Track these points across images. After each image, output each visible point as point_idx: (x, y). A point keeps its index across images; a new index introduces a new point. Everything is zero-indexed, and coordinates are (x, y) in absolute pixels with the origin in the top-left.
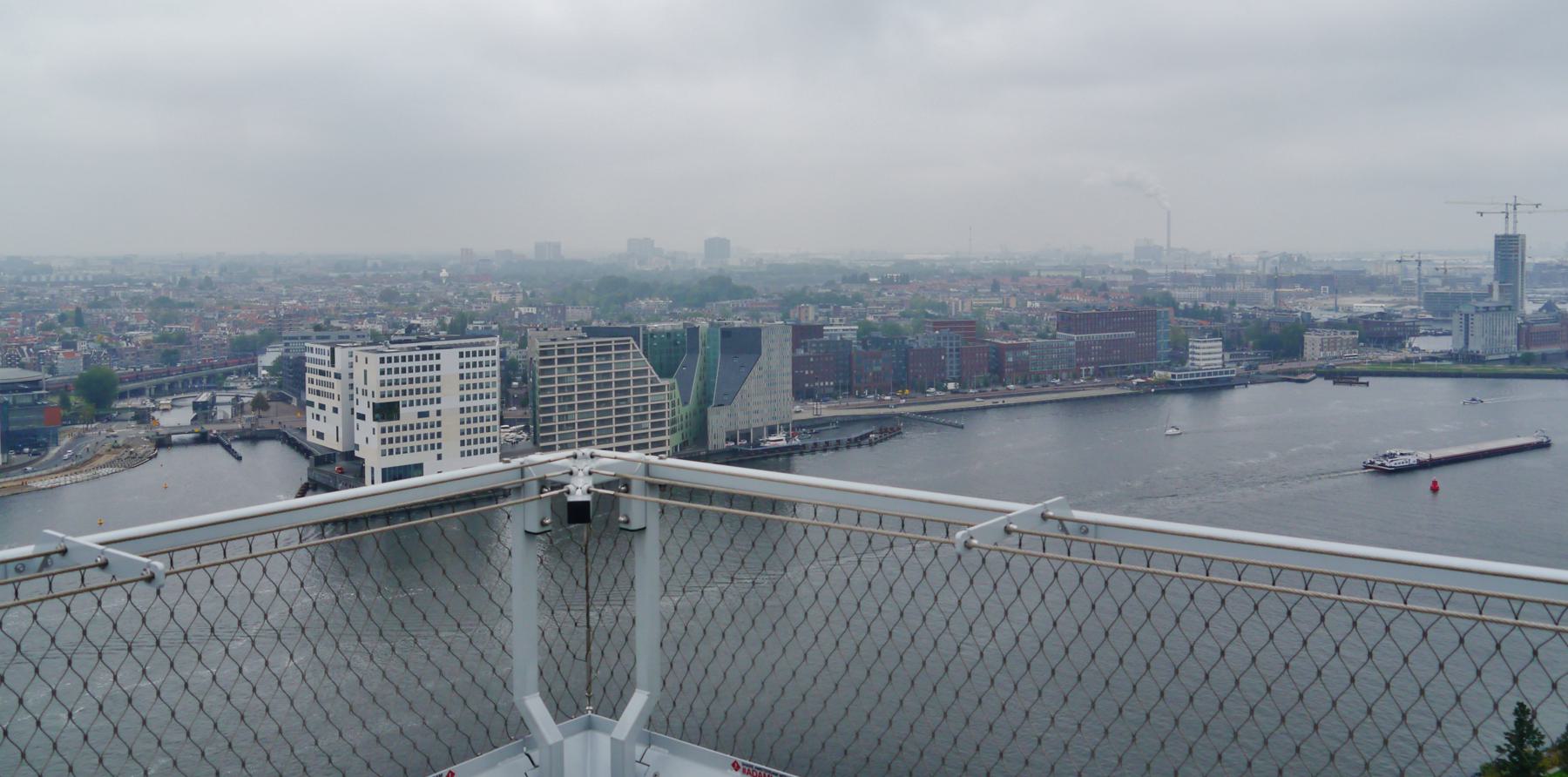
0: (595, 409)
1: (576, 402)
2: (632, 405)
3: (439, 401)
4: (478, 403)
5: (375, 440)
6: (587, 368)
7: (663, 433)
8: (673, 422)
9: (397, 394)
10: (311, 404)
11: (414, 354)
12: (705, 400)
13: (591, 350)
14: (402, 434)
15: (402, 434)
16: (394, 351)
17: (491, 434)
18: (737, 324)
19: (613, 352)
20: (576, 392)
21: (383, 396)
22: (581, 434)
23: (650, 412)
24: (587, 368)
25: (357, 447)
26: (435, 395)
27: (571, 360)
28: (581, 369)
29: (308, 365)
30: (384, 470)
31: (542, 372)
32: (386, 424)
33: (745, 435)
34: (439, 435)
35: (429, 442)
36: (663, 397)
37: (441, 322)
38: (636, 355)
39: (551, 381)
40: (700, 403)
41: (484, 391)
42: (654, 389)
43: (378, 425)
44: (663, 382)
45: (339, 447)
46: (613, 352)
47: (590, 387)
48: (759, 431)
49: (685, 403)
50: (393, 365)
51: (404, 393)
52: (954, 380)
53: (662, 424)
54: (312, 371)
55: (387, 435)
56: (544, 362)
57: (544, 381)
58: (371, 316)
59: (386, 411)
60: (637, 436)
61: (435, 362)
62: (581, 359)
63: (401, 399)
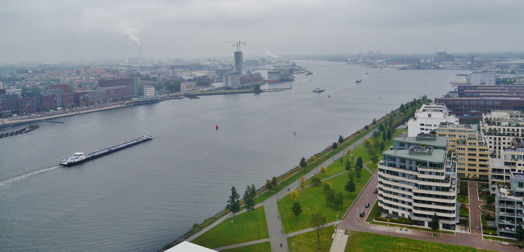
52: (60, 106)
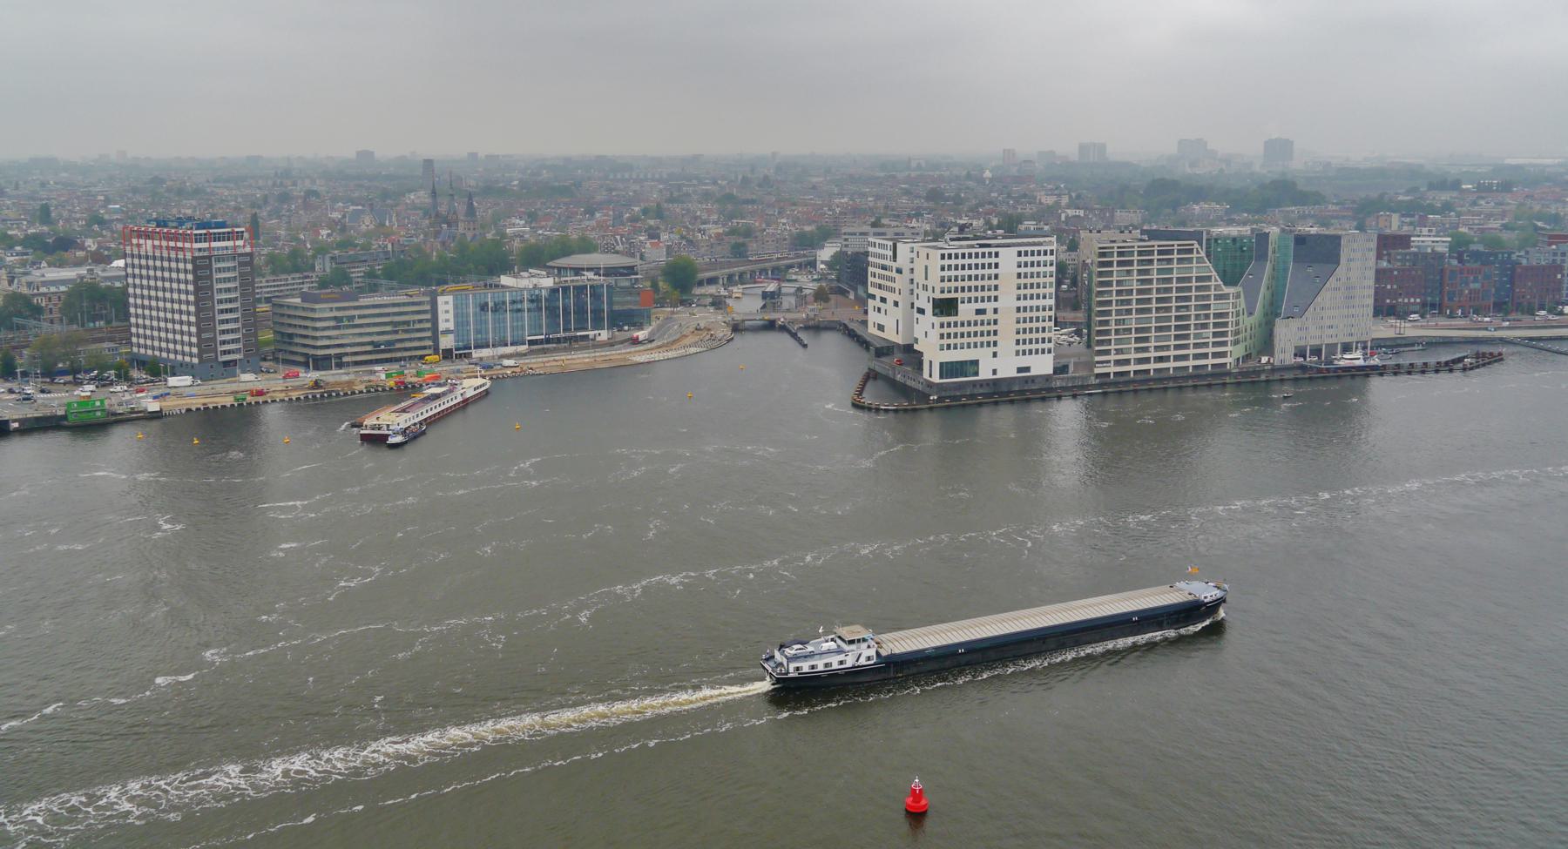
0: (1154, 314)
1: (1134, 306)
2: (1193, 312)
3: (996, 299)
4: (1035, 303)
5: (934, 334)
6: (1147, 272)
7: (1224, 344)
8: (1237, 333)
9: (956, 290)
10: (873, 297)
11: (973, 251)
12: (1272, 313)
13: (1152, 253)
14: (959, 330)
15: (959, 330)
16: (954, 248)
17: (1046, 335)
19: (1176, 256)
20: (1135, 296)
22: (1138, 340)
23: (1212, 320)
24: (1147, 272)
25: (916, 340)
26: (993, 293)
27: (1130, 263)
29: (871, 259)
31: (1101, 274)
32: (946, 319)
33: (1317, 351)
34: (995, 333)
38: (1199, 260)
39: (1109, 284)
40: (1266, 315)
42: (1218, 297)
43: (937, 320)
44: (1226, 290)
45: (899, 340)
46: (1176, 256)
47: (1149, 291)
48: (1332, 348)
49: (1251, 314)
50: (953, 262)
51: (963, 289)
53: (1224, 334)
54: (875, 265)
55: (946, 330)
56: (1102, 264)
57: (1102, 284)
59: (945, 307)
60: (1196, 346)
61: (993, 260)
62: (1141, 262)
63: (959, 295)
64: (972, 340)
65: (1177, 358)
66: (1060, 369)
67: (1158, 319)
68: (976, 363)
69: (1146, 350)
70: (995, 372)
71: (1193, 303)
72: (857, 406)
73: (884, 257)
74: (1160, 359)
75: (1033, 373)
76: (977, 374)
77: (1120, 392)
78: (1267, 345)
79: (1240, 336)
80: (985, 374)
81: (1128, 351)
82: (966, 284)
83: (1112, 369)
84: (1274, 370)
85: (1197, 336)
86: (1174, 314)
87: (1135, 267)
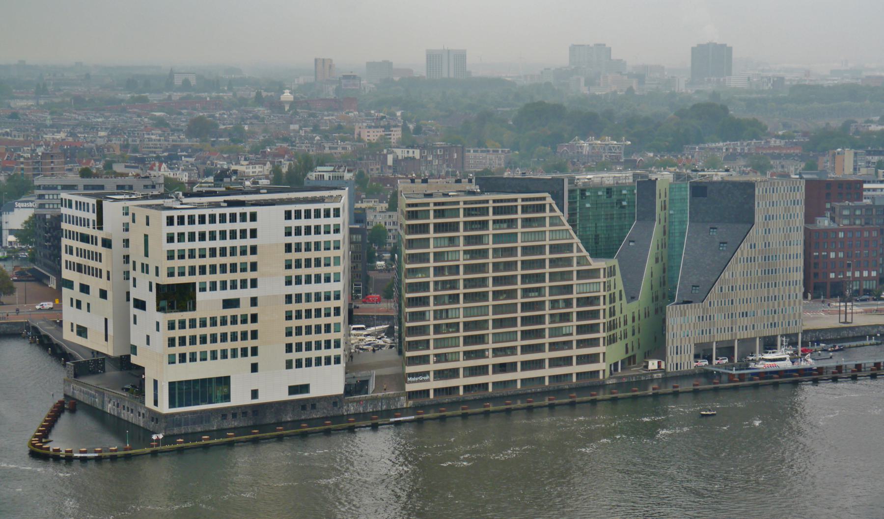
0: (491, 302)
1: (461, 290)
2: (547, 298)
3: (254, 283)
4: (313, 288)
5: (159, 340)
6: (479, 239)
7: (594, 342)
8: (612, 326)
9: (192, 271)
11: (217, 211)
12: (664, 295)
13: (485, 211)
14: (199, 331)
15: (199, 331)
16: (187, 207)
17: (332, 336)
18: (718, 175)
19: (520, 215)
20: (462, 276)
21: (171, 274)
22: (468, 340)
23: (575, 309)
24: (479, 239)
25: (134, 349)
26: (249, 275)
27: (454, 227)
28: (469, 240)
29: (65, 226)
30: (171, 384)
31: (411, 244)
32: (177, 316)
33: (726, 350)
34: (254, 334)
35: (239, 344)
36: (596, 287)
37: (276, 171)
38: (555, 221)
39: (424, 258)
40: (655, 299)
41: (322, 270)
42: (581, 274)
43: (164, 318)
44: (600, 264)
45: (108, 349)
46: (520, 215)
47: (482, 268)
48: (747, 344)
49: (632, 298)
50: (186, 229)
51: (203, 270)
53: (593, 328)
54: (71, 235)
55: (177, 333)
56: (412, 229)
57: (413, 258)
58: (171, 159)
59: (175, 297)
60: (554, 346)
61: (248, 225)
62: (468, 226)
63: (197, 279)
64: (219, 346)
65: (526, 365)
66: (355, 388)
67: (497, 309)
68: (225, 381)
69: (481, 354)
70: (255, 394)
71: (547, 284)
72: (38, 454)
73: (84, 222)
74: (502, 368)
75: (314, 393)
76: (227, 398)
77: (443, 419)
78: (656, 344)
79: (618, 331)
80: (239, 397)
81: (455, 357)
82: (208, 261)
83: (433, 385)
84: (667, 378)
85: (554, 332)
86: (519, 300)
87: (462, 233)
